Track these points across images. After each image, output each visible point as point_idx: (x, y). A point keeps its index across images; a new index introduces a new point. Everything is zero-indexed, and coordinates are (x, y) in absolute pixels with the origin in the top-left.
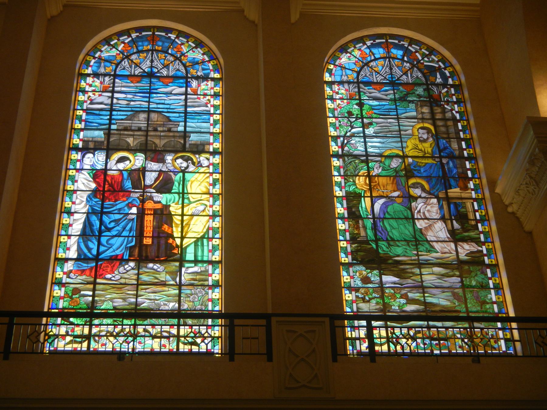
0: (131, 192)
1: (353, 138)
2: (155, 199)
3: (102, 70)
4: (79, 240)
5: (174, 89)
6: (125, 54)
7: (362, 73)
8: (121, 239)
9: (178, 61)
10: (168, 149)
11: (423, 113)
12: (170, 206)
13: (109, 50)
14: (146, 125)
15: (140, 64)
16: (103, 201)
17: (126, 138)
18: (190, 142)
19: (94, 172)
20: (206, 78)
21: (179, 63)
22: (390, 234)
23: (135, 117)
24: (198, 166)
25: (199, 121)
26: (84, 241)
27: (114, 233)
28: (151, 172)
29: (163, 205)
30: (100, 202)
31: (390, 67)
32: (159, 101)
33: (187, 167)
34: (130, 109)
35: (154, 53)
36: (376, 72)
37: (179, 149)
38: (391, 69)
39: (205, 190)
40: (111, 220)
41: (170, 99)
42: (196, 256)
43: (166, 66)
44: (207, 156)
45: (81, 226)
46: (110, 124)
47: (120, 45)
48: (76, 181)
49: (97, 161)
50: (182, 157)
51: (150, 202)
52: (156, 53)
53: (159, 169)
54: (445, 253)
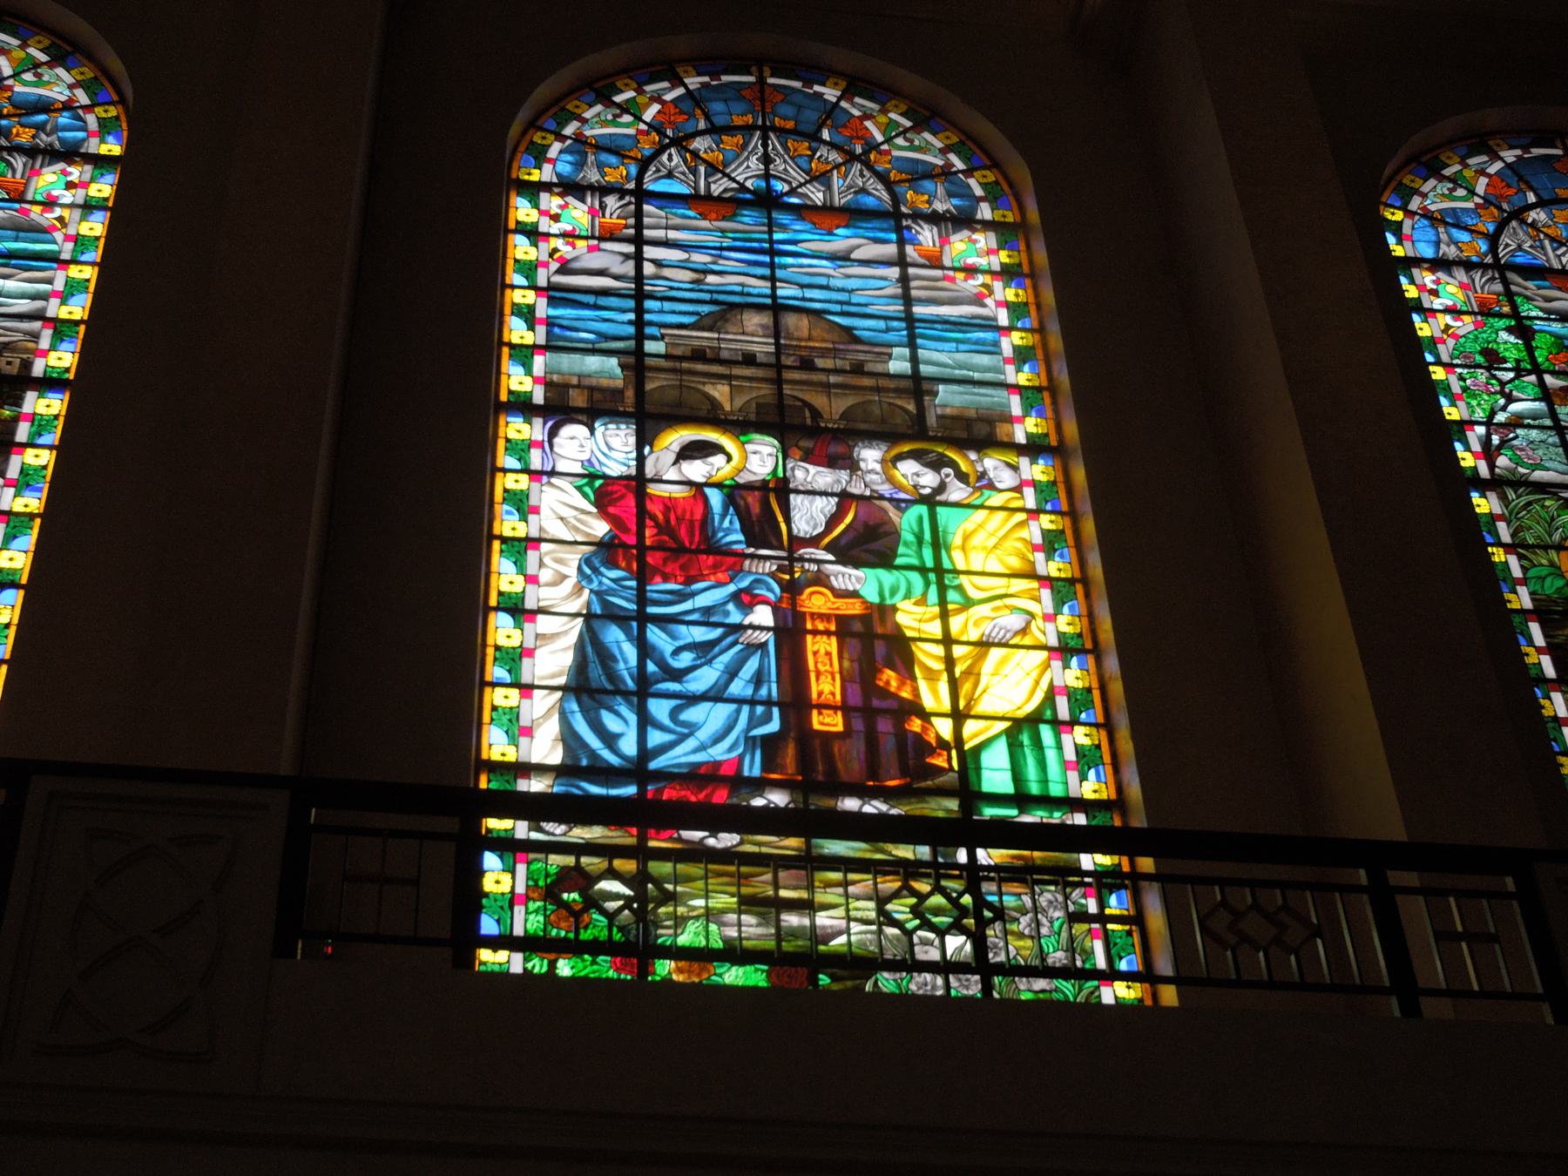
0: (745, 556)
1: (1520, 431)
3: (593, 176)
4: (566, 705)
5: (859, 246)
6: (669, 132)
8: (722, 712)
9: (857, 166)
10: (863, 426)
12: (894, 609)
13: (610, 117)
14: (772, 349)
15: (726, 165)
16: (643, 577)
17: (704, 383)
18: (939, 411)
19: (598, 483)
20: (964, 220)
21: (861, 171)
23: (727, 320)
24: (980, 488)
25: (962, 347)
26: (584, 711)
28: (811, 497)
32: (807, 280)
33: (942, 487)
34: (707, 296)
35: (772, 135)
36: (1552, 239)
37: (902, 430)
39: (1016, 563)
40: (681, 643)
41: (848, 276)
43: (822, 178)
44: (1012, 458)
45: (568, 659)
47: (647, 106)
48: (535, 510)
49: (605, 450)
50: (916, 455)
51: (813, 593)
52: (777, 137)
53: (837, 489)
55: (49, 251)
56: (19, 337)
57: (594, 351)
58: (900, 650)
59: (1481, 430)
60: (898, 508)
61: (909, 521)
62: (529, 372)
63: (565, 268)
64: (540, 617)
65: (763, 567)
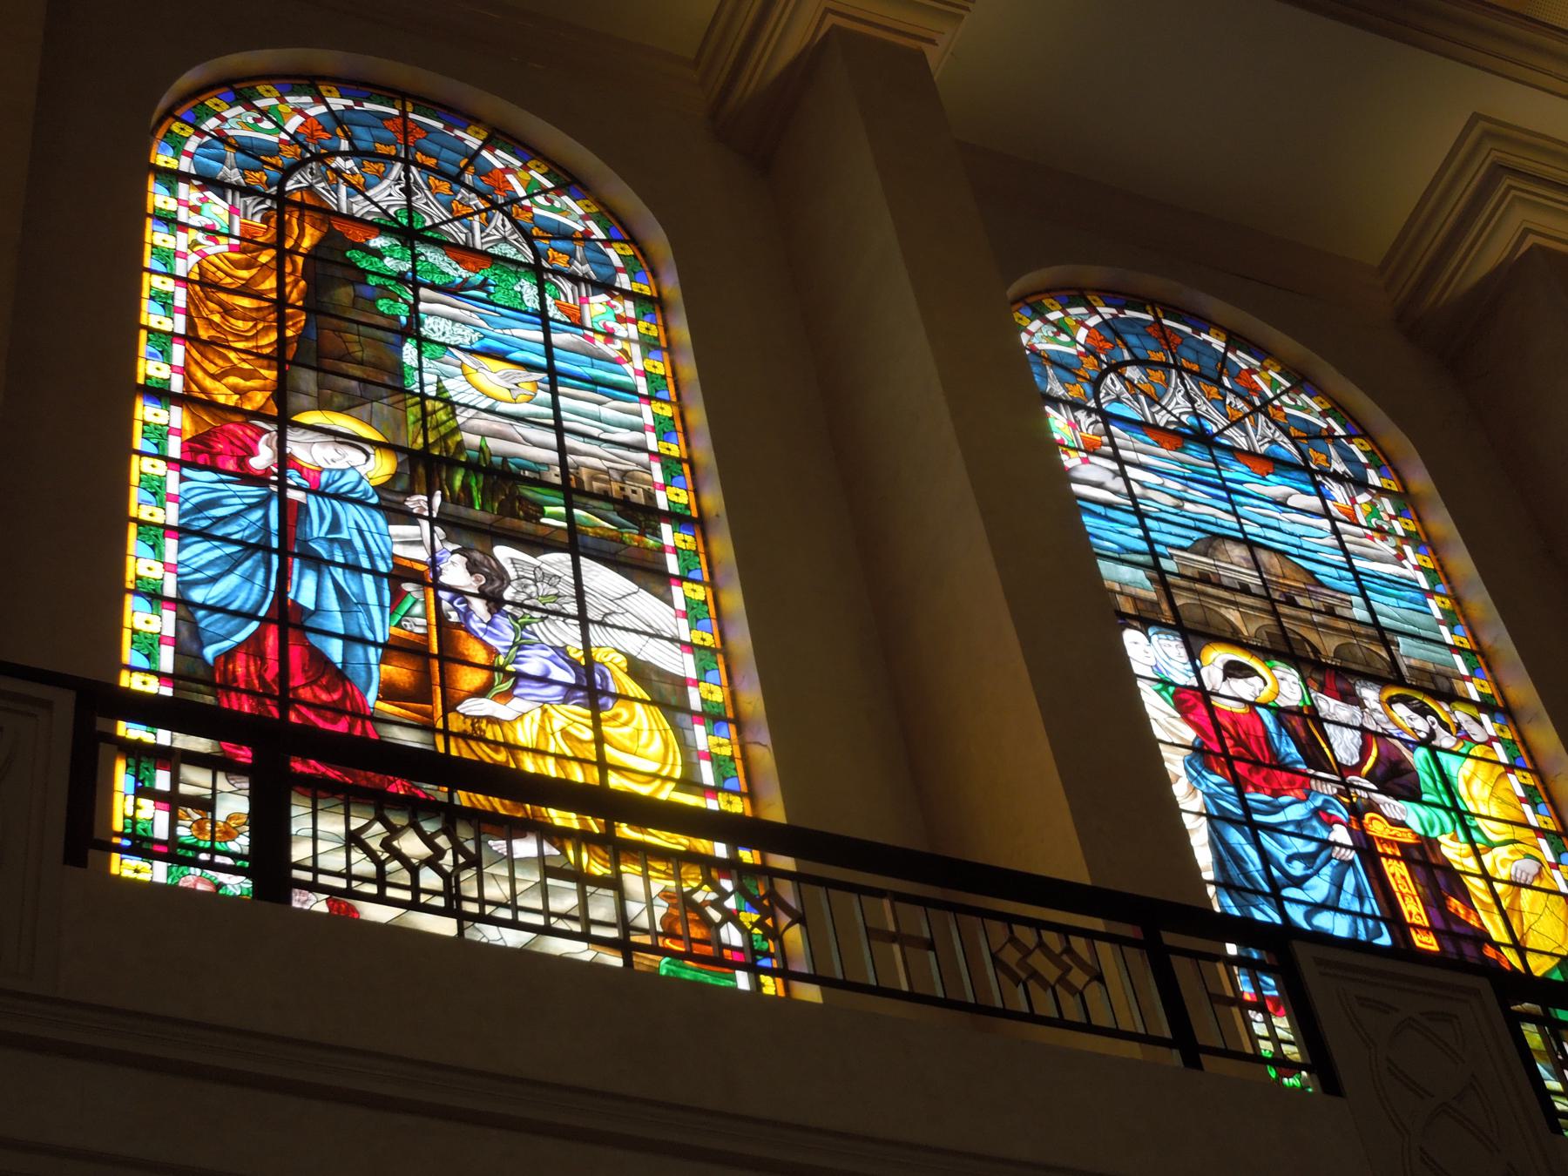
32: (1263, 520)
55: (626, 383)
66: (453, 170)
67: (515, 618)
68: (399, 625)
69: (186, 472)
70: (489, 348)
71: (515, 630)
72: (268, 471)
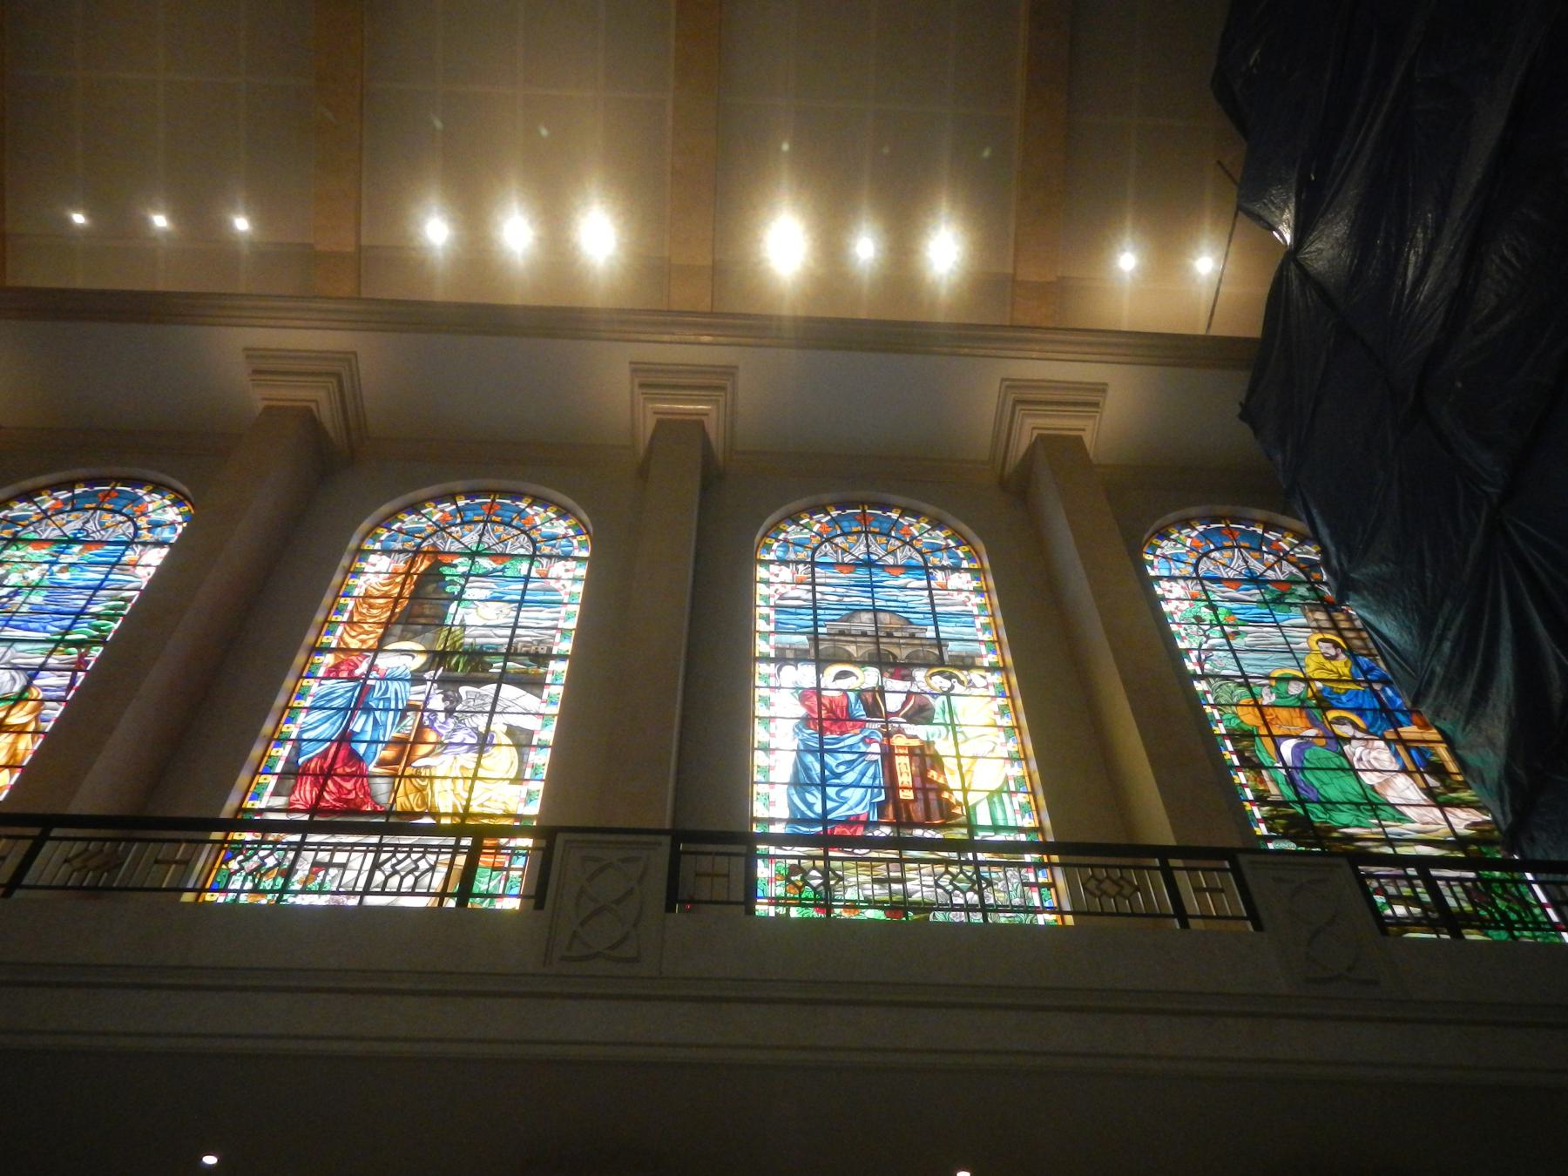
1: (1215, 653)
2: (908, 732)
3: (792, 556)
6: (825, 536)
7: (1201, 566)
9: (907, 547)
10: (916, 662)
11: (1316, 620)
12: (934, 742)
14: (874, 629)
15: (850, 549)
16: (821, 733)
18: (949, 653)
19: (800, 691)
20: (956, 568)
22: (1321, 791)
23: (854, 617)
25: (958, 625)
27: (849, 778)
29: (922, 742)
30: (817, 735)
31: (1244, 558)
32: (888, 598)
34: (844, 607)
36: (1223, 565)
37: (932, 662)
38: (1246, 562)
39: (989, 722)
40: (839, 762)
42: (993, 818)
43: (893, 553)
44: (983, 673)
46: (816, 626)
47: (815, 525)
48: (772, 705)
50: (940, 673)
53: (906, 690)
54: (1427, 823)
56: (547, 637)
57: (795, 633)
58: (937, 762)
59: (1196, 653)
60: (933, 697)
61: (938, 703)
62: (768, 643)
63: (782, 598)
64: (777, 752)
65: (874, 726)
66: (507, 520)
67: (457, 718)
68: (399, 732)
69: (323, 682)
70: (495, 597)
71: (455, 724)
72: (363, 674)
